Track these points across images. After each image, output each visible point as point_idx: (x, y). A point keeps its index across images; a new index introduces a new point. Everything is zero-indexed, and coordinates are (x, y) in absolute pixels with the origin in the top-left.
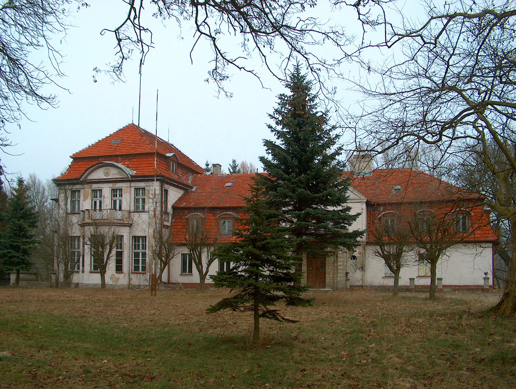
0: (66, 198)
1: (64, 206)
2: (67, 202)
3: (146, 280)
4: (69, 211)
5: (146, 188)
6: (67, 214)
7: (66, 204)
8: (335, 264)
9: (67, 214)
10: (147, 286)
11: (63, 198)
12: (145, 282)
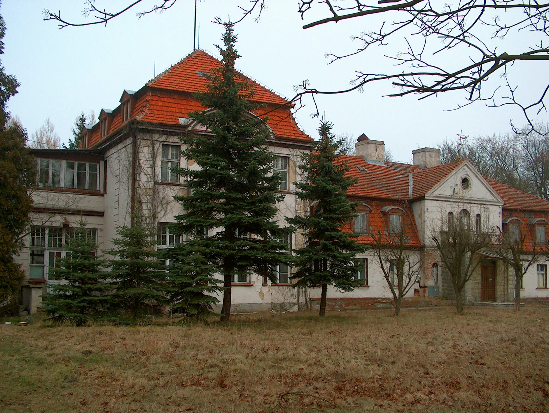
0: (154, 156)
1: (149, 171)
2: (154, 163)
3: (292, 295)
4: (159, 179)
5: (291, 157)
6: (156, 183)
7: (153, 167)
8: (506, 275)
9: (156, 183)
10: (294, 304)
11: (148, 156)
12: (291, 299)
